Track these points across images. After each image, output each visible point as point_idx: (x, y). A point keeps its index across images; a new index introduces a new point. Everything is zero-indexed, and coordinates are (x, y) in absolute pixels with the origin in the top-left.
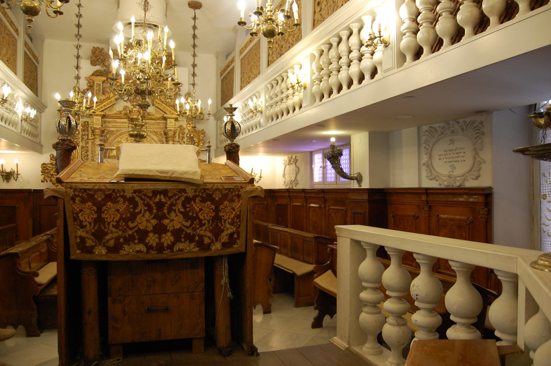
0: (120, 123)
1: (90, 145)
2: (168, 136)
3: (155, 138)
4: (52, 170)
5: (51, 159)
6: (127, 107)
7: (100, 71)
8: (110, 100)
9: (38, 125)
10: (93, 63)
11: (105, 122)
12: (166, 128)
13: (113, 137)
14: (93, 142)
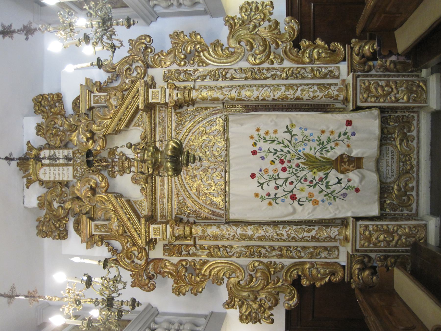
0: (163, 190)
1: (206, 243)
2: (182, 100)
3: (188, 125)
4: (251, 306)
5: (233, 307)
6: (133, 179)
7: (74, 224)
8: (119, 209)
9: (175, 319)
10: (63, 235)
11: (163, 216)
12: (166, 104)
13: (190, 202)
14: (201, 238)
